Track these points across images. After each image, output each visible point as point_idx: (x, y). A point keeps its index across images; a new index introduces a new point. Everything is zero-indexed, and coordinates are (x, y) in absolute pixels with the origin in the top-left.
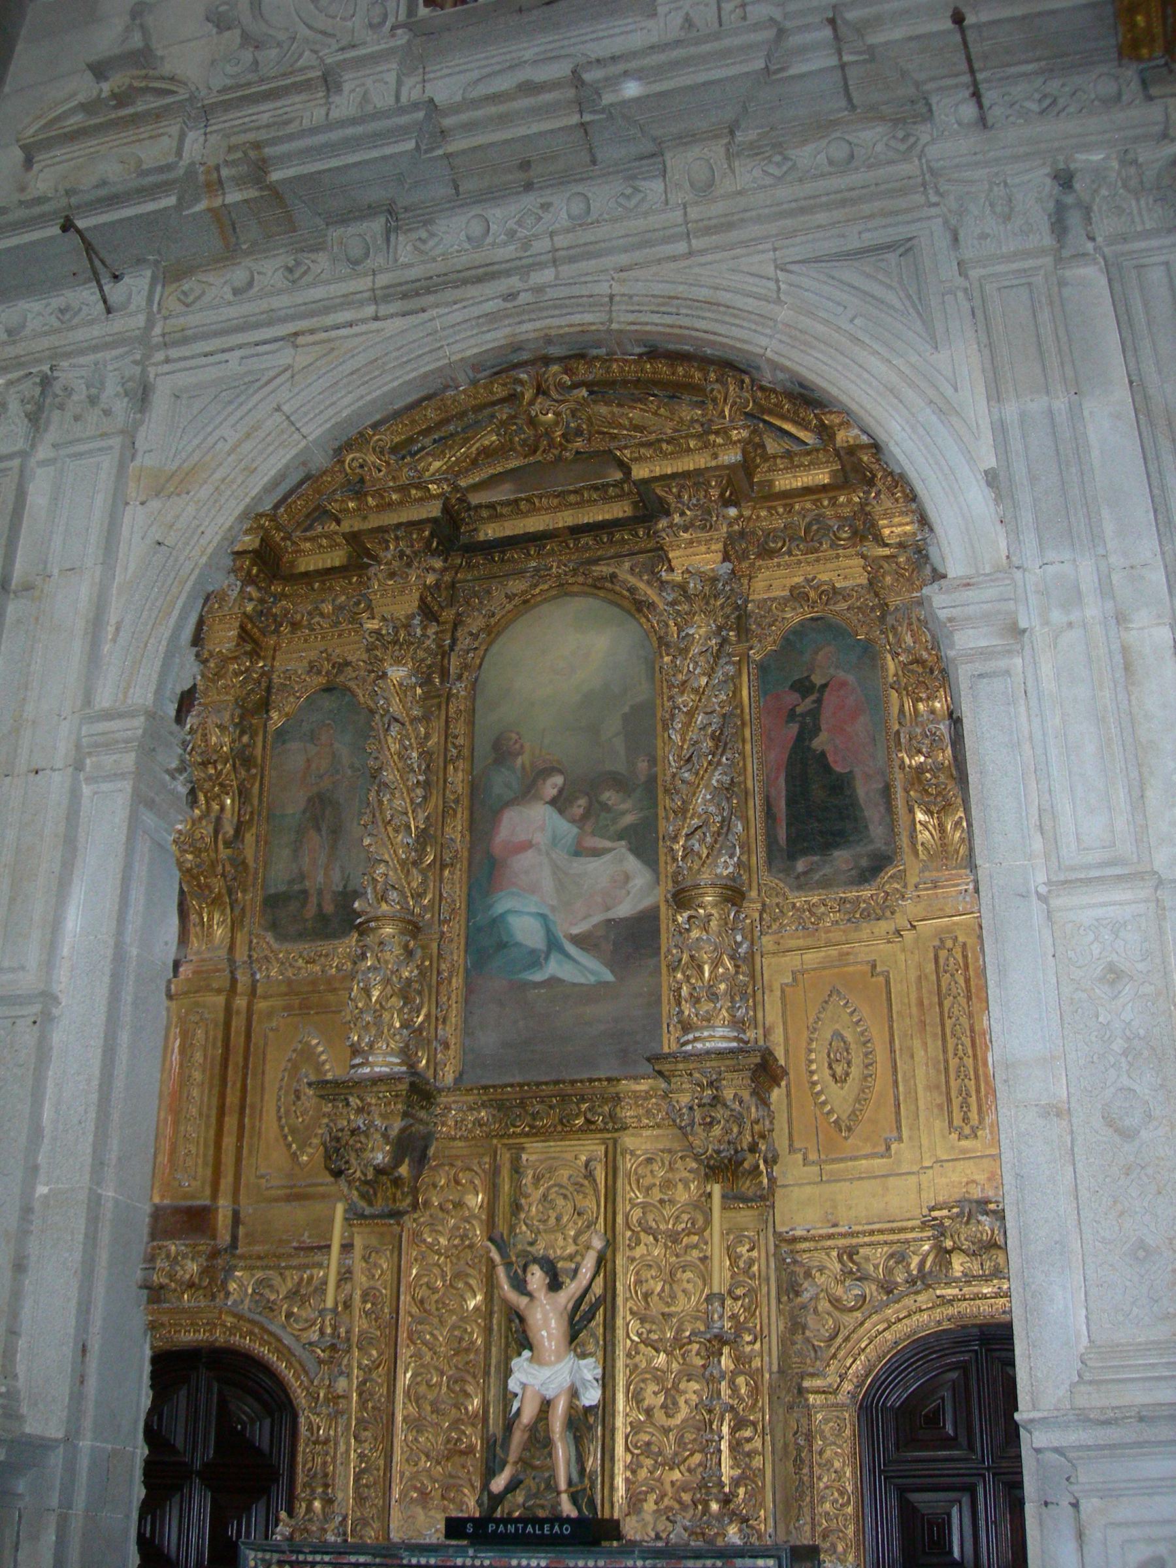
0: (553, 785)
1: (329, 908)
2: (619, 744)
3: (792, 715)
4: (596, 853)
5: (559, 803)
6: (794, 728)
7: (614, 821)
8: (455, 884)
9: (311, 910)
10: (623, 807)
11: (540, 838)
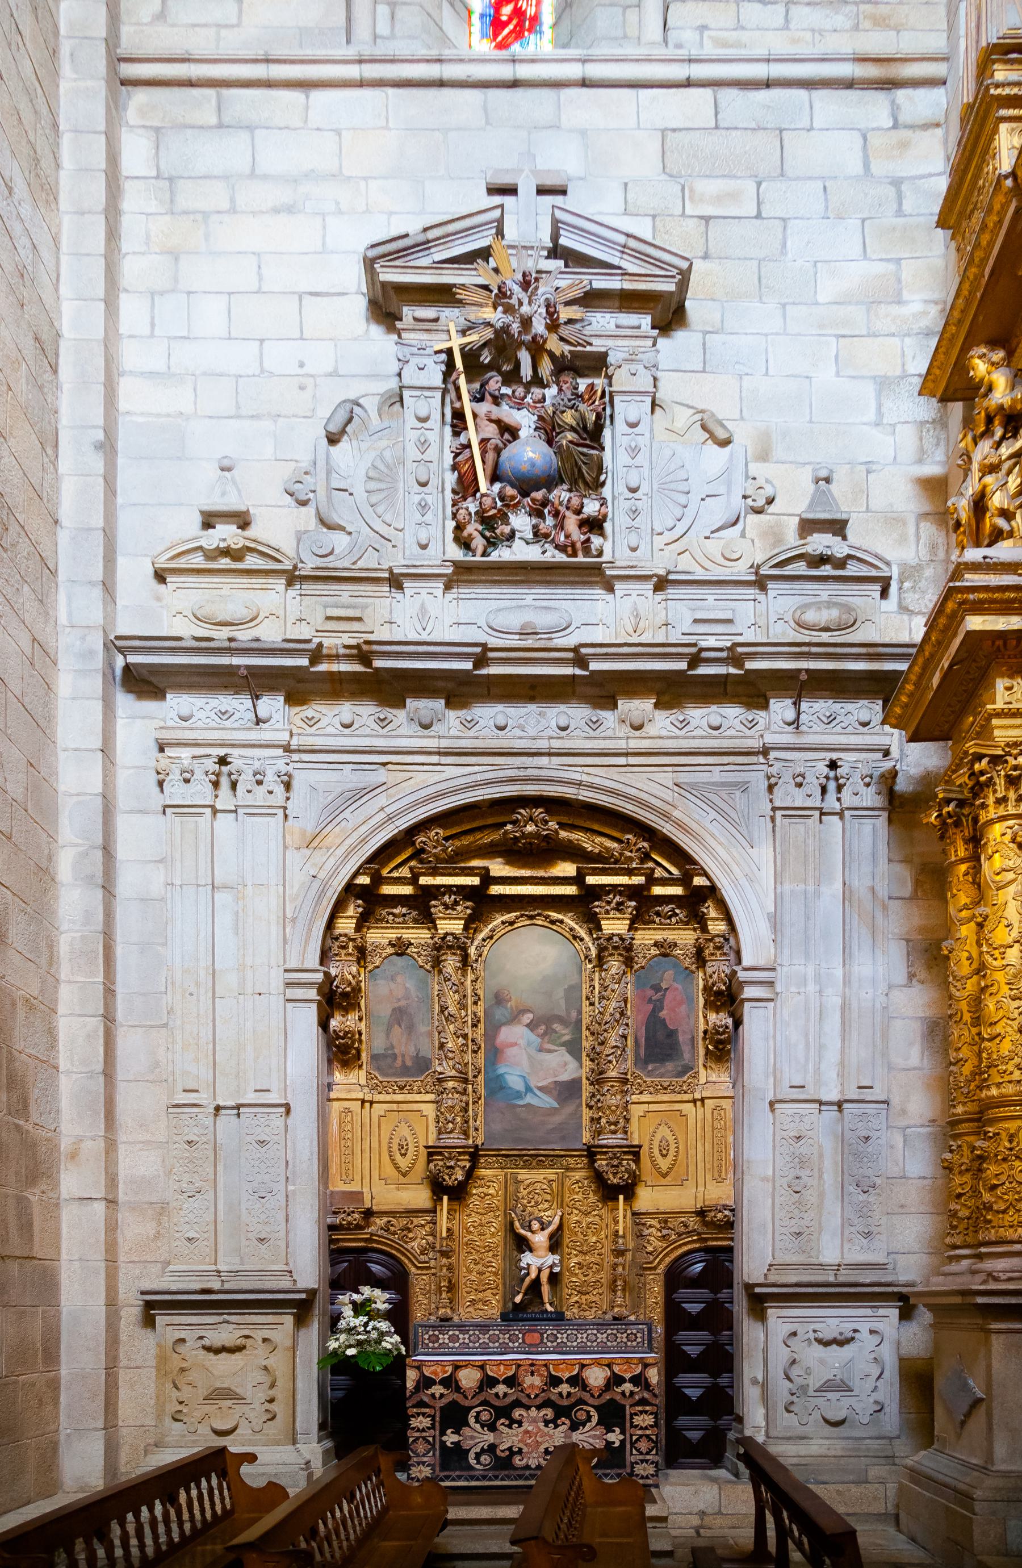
0: (527, 1018)
1: (409, 1063)
2: (562, 1003)
3: (650, 1000)
4: (550, 1051)
5: (531, 1026)
6: (651, 1006)
7: (559, 1038)
8: (481, 1060)
9: (399, 1062)
10: (563, 1032)
11: (522, 1042)
